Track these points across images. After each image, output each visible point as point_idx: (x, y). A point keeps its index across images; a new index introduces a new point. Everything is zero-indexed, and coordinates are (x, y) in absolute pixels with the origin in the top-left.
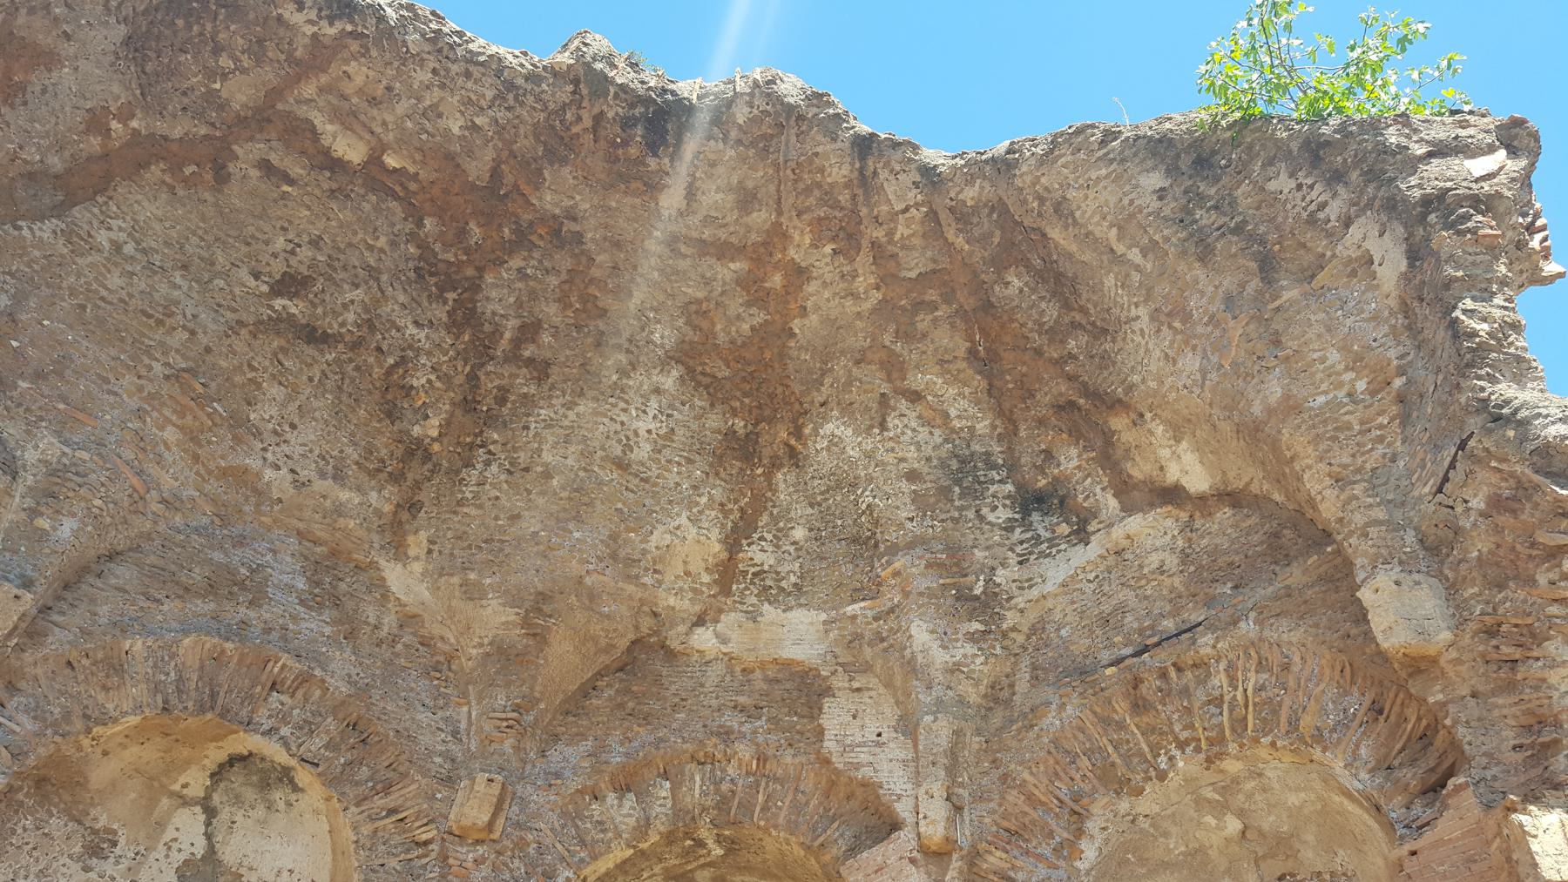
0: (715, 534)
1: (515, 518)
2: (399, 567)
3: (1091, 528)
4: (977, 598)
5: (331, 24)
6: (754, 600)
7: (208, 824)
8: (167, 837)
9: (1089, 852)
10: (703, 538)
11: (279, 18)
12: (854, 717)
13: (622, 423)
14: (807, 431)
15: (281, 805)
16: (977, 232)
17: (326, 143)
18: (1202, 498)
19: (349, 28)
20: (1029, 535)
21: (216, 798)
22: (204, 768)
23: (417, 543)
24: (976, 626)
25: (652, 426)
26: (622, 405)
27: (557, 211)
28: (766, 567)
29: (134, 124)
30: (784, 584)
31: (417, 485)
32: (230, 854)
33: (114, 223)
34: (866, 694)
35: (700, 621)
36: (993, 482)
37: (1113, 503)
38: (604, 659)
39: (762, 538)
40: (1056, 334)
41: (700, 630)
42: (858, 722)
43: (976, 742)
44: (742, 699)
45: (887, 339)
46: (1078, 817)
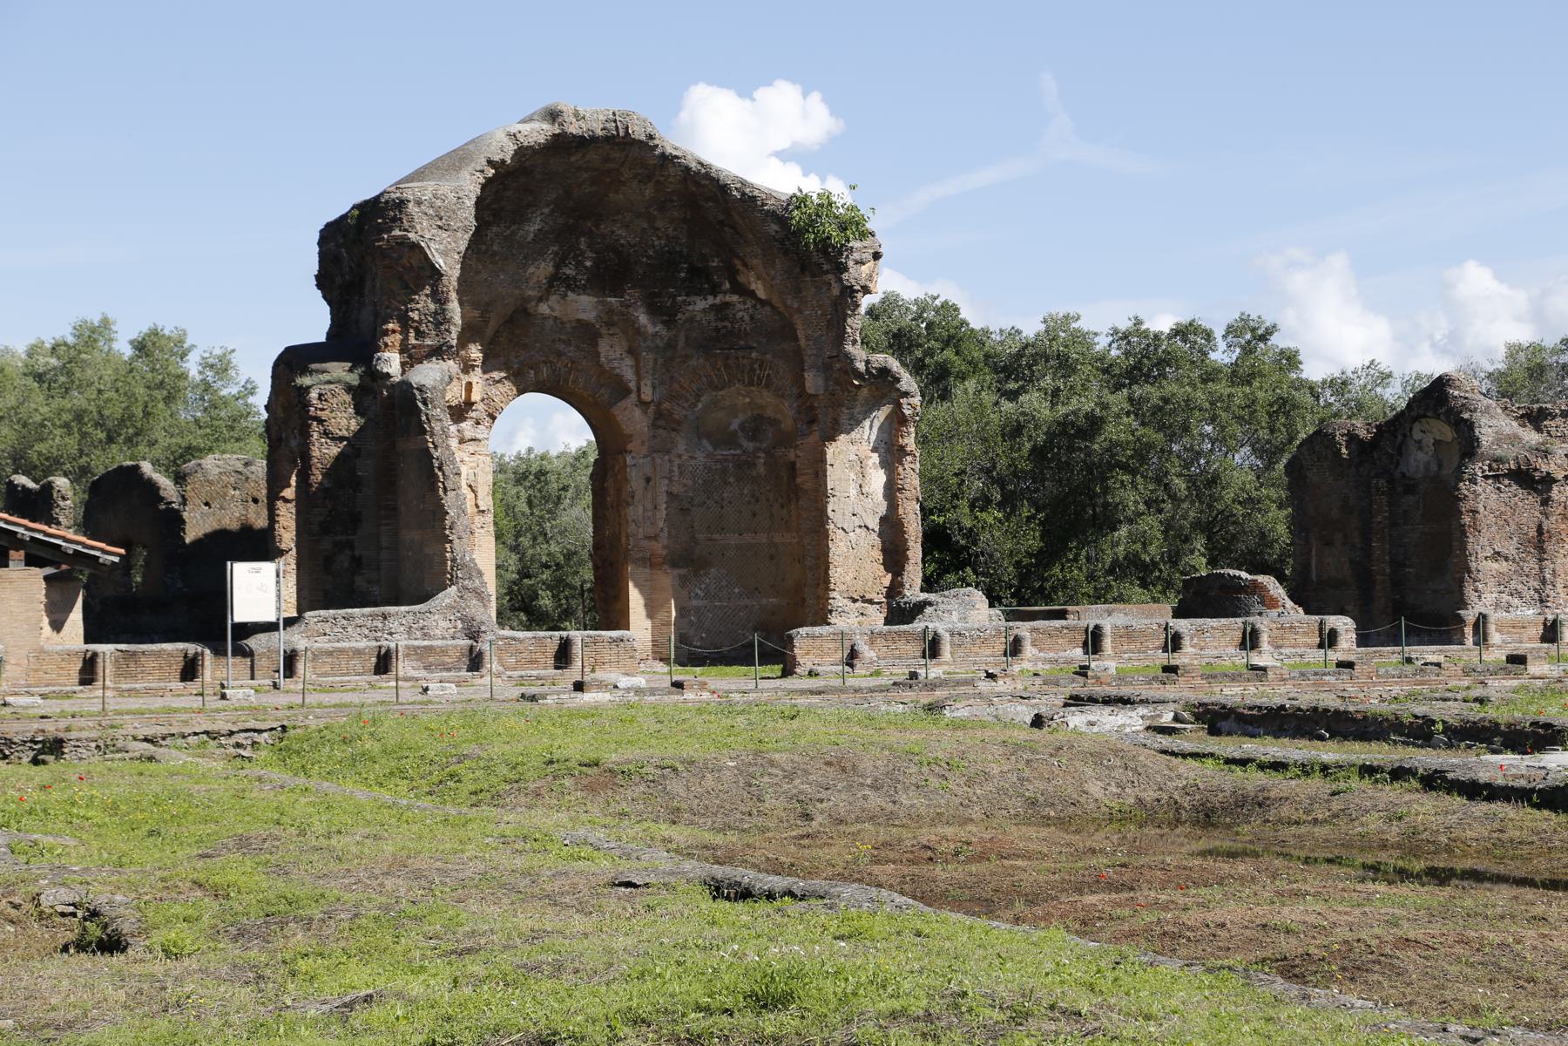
1: (478, 272)
9: (700, 405)
35: (540, 300)
40: (721, 223)
43: (660, 361)
46: (698, 397)
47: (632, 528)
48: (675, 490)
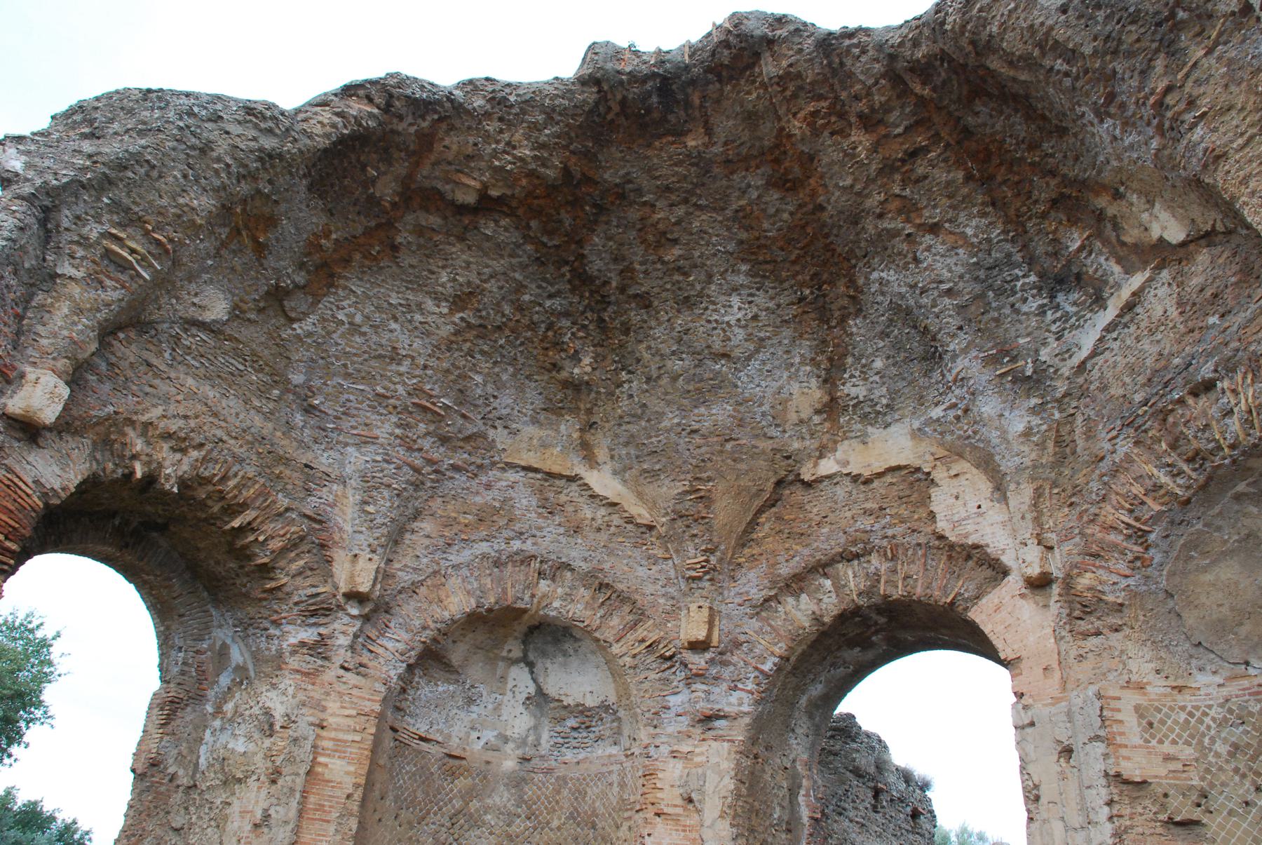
0: (814, 382)
2: (595, 472)
3: (1106, 295)
4: (1029, 377)
5: (424, 120)
6: (859, 426)
7: (532, 673)
8: (510, 686)
10: (806, 390)
11: (392, 131)
12: (957, 498)
13: (716, 321)
14: (861, 281)
15: (571, 652)
16: (938, 81)
17: (450, 198)
18: (1183, 244)
19: (436, 117)
20: (1058, 314)
21: (531, 656)
22: (516, 638)
23: (602, 454)
24: (1034, 401)
25: (739, 316)
26: (711, 307)
27: (618, 181)
28: (861, 399)
29: (334, 236)
30: (878, 408)
31: (589, 412)
32: (551, 689)
33: (345, 303)
34: (962, 478)
36: (1017, 278)
37: (1117, 269)
38: (758, 503)
39: (852, 376)
41: (823, 462)
42: (960, 502)
44: (868, 505)
45: (897, 190)
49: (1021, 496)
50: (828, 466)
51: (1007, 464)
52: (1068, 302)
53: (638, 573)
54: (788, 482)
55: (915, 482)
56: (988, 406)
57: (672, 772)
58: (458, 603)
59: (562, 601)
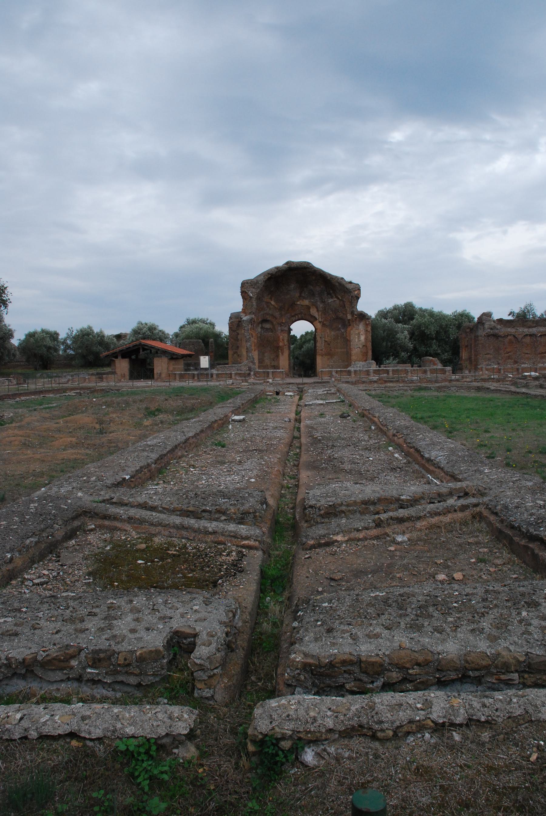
47: (317, 348)
48: (326, 340)
49: (320, 313)
50: (298, 303)
51: (319, 309)
52: (329, 296)
53: (277, 314)
54: (293, 305)
55: (308, 308)
56: (318, 303)
57: (281, 337)
58: (260, 320)
59: (269, 318)
